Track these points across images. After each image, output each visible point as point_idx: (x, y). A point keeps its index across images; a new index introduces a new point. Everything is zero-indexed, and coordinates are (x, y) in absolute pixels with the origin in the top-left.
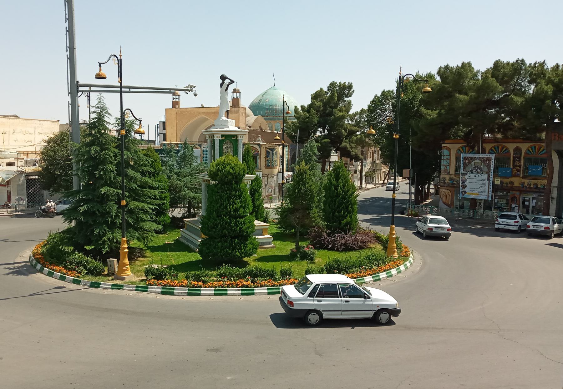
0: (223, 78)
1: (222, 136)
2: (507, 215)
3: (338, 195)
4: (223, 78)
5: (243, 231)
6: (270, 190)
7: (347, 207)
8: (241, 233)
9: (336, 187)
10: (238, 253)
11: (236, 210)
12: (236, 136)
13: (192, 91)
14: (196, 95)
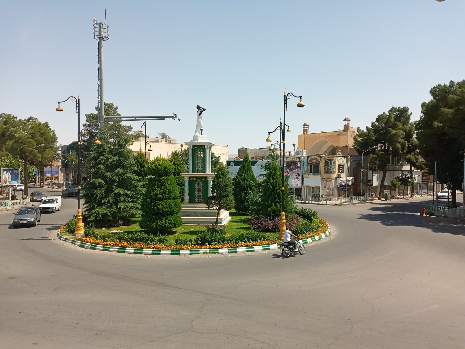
0: (198, 108)
1: (194, 146)
2: (190, 195)
3: (269, 188)
4: (198, 108)
5: (160, 210)
6: (328, 191)
7: (275, 199)
8: (159, 211)
9: (267, 184)
10: (154, 226)
11: (156, 195)
12: (204, 146)
13: (176, 117)
14: (179, 120)
